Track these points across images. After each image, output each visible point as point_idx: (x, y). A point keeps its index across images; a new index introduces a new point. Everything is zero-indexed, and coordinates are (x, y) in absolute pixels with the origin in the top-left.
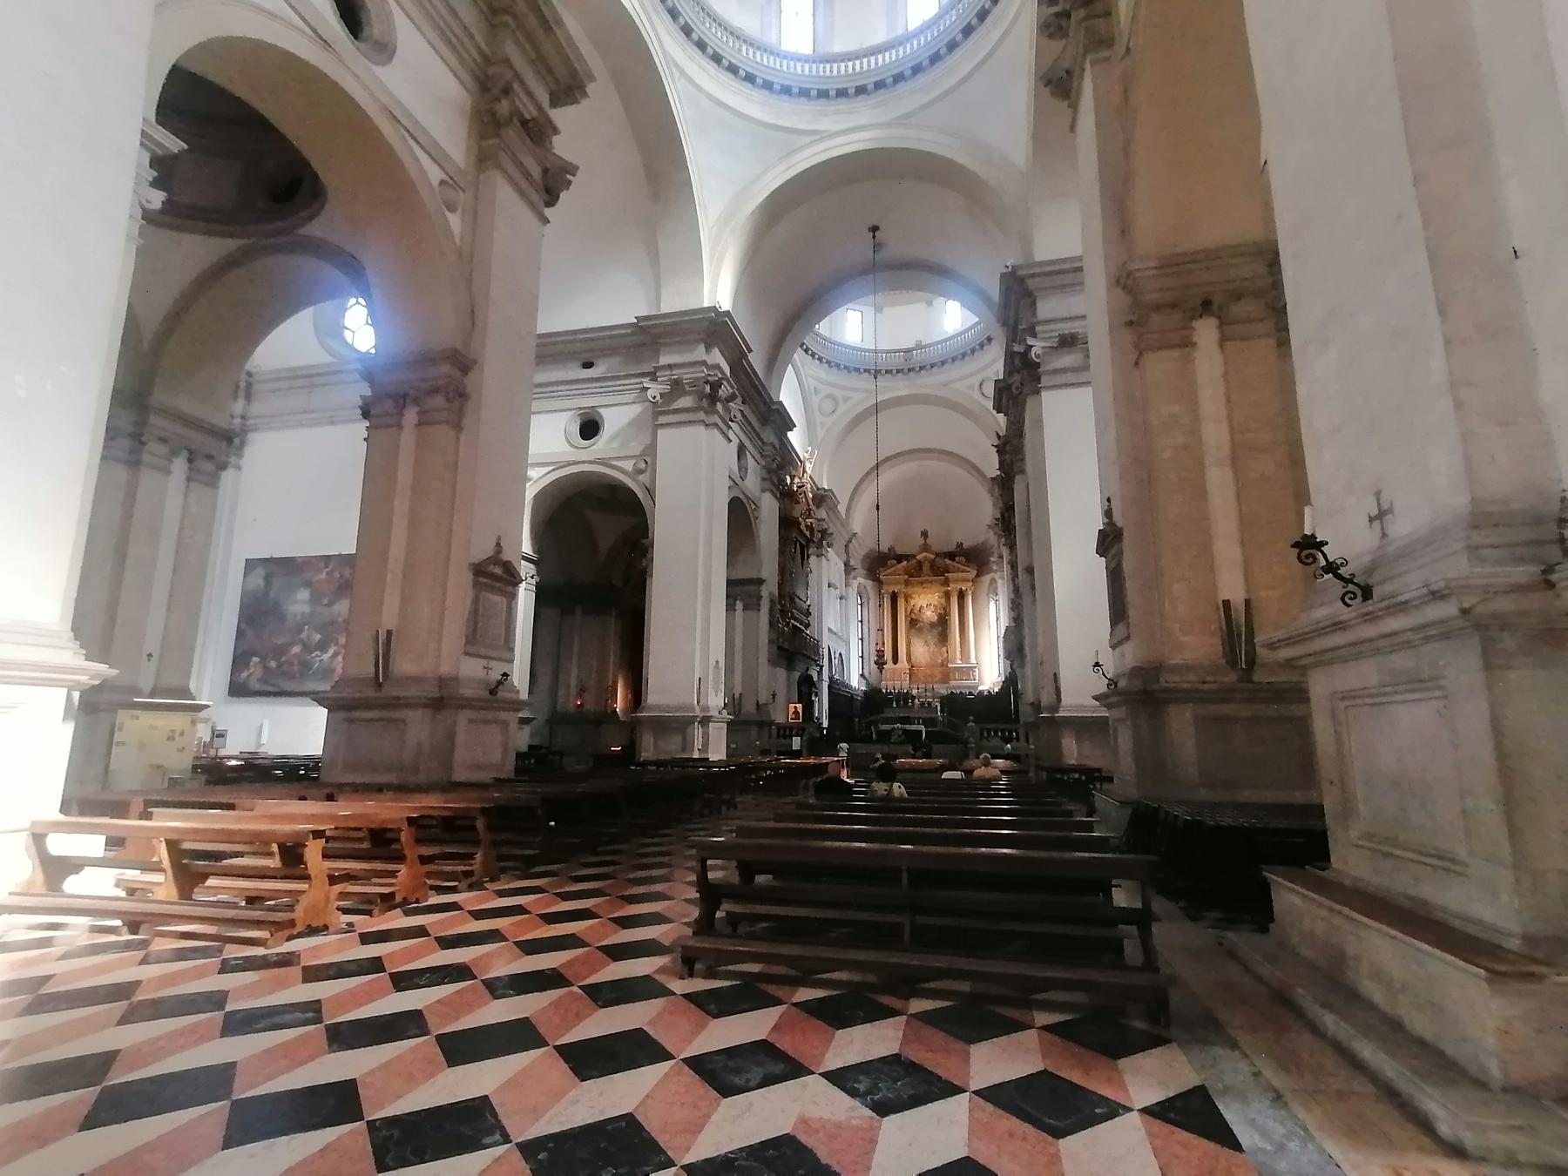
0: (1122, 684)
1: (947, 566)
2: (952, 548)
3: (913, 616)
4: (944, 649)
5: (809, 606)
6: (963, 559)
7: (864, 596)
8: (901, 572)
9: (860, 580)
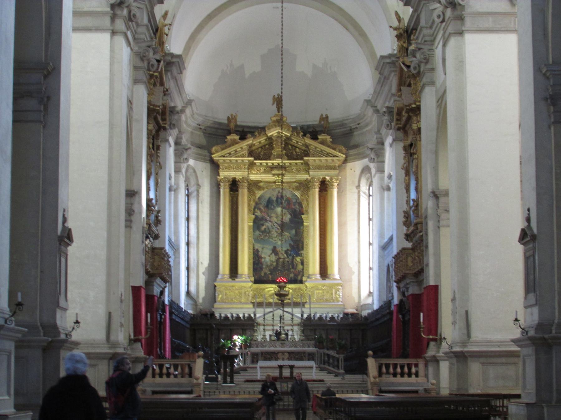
0: (532, 333)
1: (307, 146)
2: (313, 119)
3: (258, 213)
4: (298, 259)
6: (328, 138)
7: (193, 182)
8: (246, 152)
9: (191, 162)
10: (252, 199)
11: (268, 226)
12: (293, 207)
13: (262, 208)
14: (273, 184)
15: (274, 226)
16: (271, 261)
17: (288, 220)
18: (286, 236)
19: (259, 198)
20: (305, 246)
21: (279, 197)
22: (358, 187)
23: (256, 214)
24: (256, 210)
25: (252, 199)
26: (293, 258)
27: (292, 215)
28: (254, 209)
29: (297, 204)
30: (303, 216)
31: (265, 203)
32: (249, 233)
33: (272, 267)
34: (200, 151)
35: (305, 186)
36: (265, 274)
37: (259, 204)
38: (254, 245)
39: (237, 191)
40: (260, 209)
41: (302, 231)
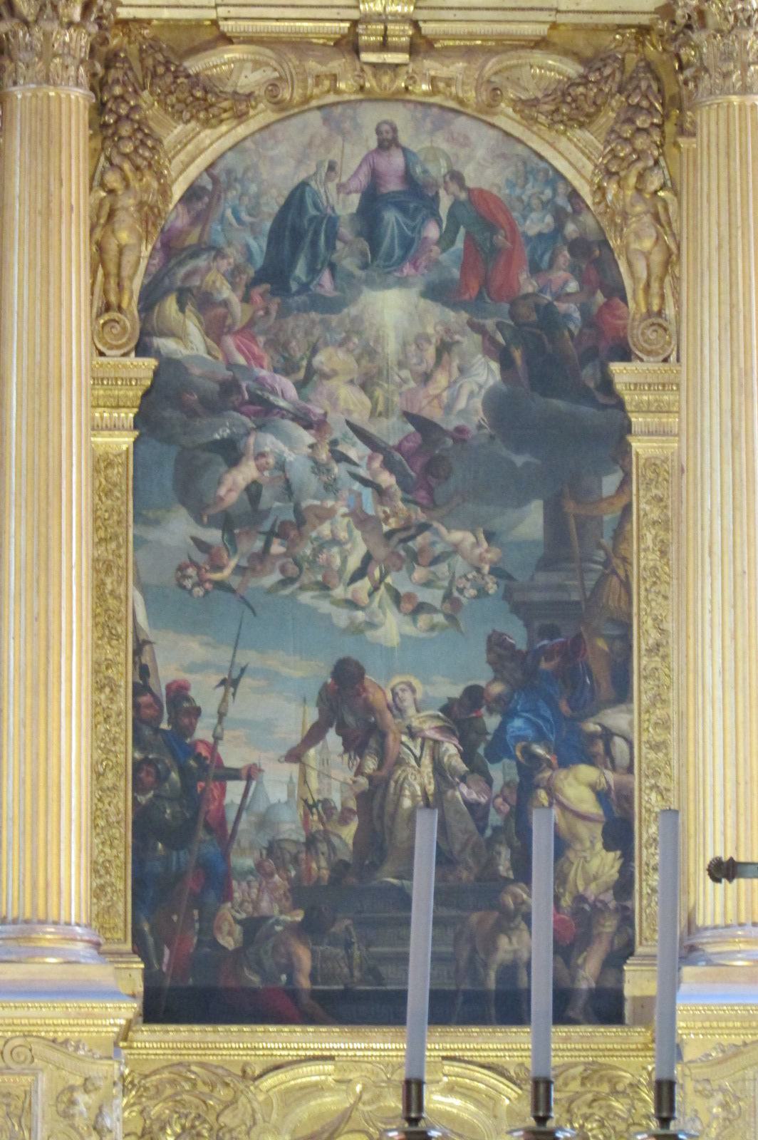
10: (128, 202)
11: (281, 466)
12: (528, 285)
13: (226, 292)
14: (338, 64)
15: (338, 469)
16: (309, 807)
17: (478, 403)
18: (460, 564)
19: (193, 194)
20: (640, 662)
21: (393, 185)
23: (168, 345)
24: (171, 305)
25: (128, 202)
26: (529, 771)
27: (517, 354)
28: (150, 299)
29: (565, 256)
30: (616, 367)
31: (259, 246)
32: (103, 530)
33: (320, 868)
36: (253, 927)
37: (195, 253)
38: (140, 646)
40: (204, 302)
41: (610, 517)
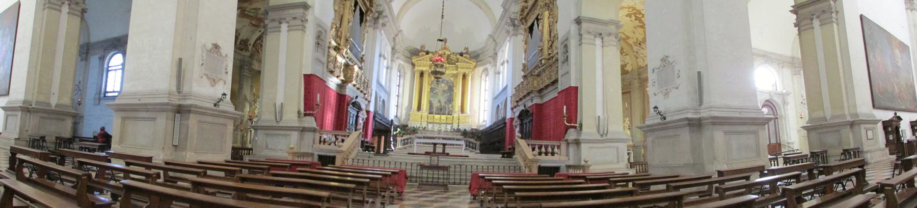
3: (433, 86)
5: (363, 55)
7: (402, 71)
22: (481, 77)
34: (407, 59)
35: (456, 76)
39: (423, 77)
